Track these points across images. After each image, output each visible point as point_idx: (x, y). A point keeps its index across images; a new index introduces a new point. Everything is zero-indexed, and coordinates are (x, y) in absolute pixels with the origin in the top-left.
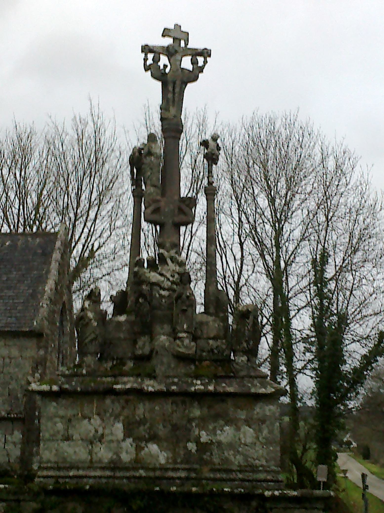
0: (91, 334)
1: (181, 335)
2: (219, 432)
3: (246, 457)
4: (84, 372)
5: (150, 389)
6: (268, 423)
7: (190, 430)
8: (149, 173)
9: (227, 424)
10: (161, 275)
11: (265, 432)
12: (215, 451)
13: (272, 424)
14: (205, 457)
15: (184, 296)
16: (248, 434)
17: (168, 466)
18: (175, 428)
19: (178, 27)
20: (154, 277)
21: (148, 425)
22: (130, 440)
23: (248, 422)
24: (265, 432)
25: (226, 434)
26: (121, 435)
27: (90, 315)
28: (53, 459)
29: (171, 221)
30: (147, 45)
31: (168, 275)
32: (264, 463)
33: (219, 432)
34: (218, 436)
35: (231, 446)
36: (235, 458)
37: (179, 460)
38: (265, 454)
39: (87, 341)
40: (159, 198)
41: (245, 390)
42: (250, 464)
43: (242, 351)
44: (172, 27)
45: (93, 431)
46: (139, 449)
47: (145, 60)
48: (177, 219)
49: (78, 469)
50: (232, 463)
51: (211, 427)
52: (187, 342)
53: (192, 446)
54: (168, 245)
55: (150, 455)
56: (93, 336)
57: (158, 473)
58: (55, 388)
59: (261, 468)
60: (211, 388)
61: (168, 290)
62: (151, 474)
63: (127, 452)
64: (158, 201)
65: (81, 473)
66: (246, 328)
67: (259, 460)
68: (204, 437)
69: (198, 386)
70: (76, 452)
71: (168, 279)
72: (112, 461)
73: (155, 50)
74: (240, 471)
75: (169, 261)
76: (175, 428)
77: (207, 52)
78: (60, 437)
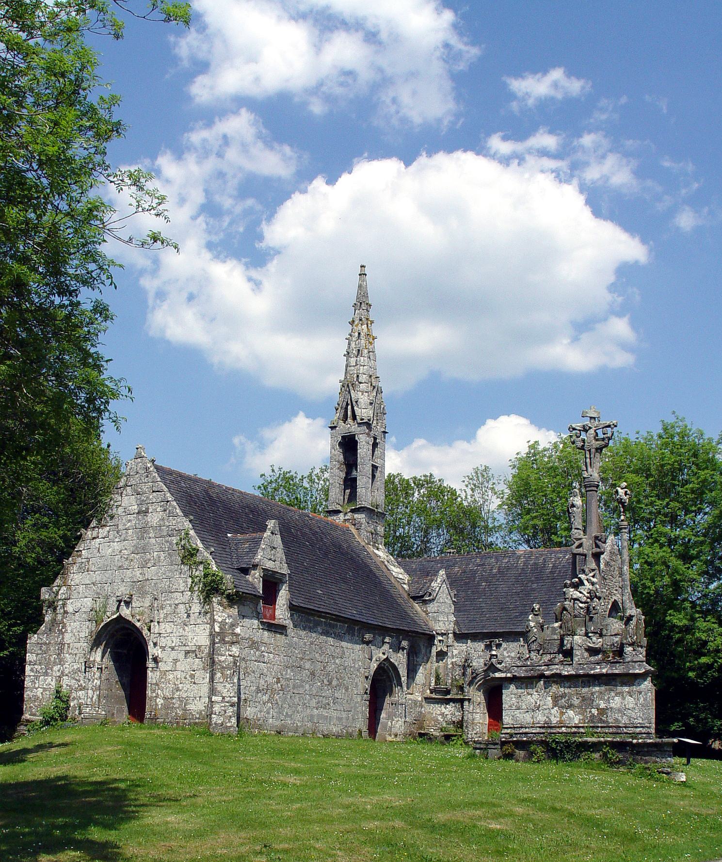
3: (630, 718)
5: (566, 673)
10: (581, 592)
13: (646, 694)
16: (630, 701)
18: (584, 699)
20: (575, 594)
22: (556, 708)
23: (630, 694)
25: (616, 702)
26: (551, 705)
27: (532, 624)
28: (511, 722)
31: (585, 593)
35: (619, 710)
40: (582, 536)
46: (562, 714)
50: (620, 722)
52: (594, 639)
53: (595, 711)
57: (574, 730)
58: (509, 675)
60: (604, 671)
61: (584, 603)
62: (569, 730)
68: (602, 705)
72: (546, 723)
75: (586, 582)
76: (584, 699)
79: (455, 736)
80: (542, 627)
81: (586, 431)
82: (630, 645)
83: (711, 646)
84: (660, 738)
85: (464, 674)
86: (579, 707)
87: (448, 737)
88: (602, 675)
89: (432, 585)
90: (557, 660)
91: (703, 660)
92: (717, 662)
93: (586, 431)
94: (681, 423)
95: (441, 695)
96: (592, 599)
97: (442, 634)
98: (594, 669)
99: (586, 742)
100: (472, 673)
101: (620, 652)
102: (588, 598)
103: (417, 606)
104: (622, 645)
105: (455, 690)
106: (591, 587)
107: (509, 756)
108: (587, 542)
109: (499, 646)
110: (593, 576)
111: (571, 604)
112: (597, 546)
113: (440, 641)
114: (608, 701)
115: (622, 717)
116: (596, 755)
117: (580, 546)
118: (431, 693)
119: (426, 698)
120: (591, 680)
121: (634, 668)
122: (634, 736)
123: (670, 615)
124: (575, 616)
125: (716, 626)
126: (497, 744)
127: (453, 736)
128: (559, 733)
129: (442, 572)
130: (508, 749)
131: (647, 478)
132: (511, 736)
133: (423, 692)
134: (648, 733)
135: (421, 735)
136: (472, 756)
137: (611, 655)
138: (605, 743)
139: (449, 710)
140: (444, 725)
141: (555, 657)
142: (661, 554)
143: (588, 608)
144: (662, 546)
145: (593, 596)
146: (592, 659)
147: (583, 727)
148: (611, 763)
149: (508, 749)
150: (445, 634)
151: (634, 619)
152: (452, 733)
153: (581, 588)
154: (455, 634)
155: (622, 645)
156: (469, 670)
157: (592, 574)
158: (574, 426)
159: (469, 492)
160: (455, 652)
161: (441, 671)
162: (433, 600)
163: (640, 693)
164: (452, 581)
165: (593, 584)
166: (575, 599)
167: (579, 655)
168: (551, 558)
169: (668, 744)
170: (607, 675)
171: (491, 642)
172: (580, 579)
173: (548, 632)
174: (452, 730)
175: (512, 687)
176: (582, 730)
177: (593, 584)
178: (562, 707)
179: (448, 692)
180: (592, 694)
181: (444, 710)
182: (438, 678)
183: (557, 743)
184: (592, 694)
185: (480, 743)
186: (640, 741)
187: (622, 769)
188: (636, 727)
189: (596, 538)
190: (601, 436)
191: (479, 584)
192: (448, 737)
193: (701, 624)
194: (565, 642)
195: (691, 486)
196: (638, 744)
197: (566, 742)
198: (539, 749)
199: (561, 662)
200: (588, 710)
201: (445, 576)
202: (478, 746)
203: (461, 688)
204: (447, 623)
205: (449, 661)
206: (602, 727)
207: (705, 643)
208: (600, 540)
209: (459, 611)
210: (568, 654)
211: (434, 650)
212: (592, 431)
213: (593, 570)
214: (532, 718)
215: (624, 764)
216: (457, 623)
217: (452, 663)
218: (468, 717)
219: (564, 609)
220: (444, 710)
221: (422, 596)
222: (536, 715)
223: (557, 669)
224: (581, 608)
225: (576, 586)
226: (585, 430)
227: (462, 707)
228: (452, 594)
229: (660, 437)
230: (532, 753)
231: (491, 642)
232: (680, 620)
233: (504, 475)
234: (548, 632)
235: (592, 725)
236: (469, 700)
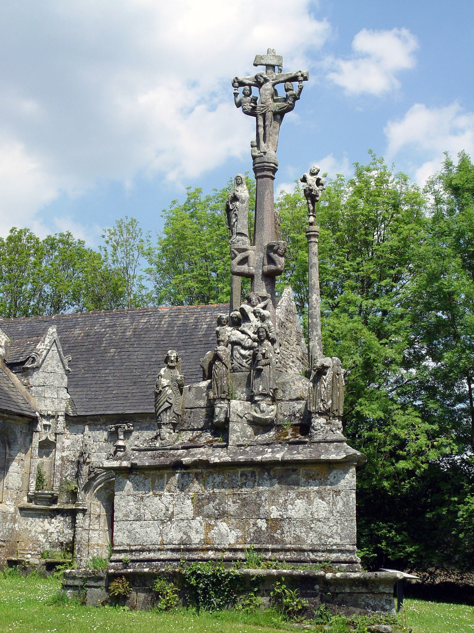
0: (164, 403)
1: (257, 398)
2: (290, 506)
3: (320, 535)
4: (158, 445)
5: (217, 460)
6: (342, 494)
7: (260, 505)
8: (234, 220)
9: (298, 497)
10: (243, 332)
11: (340, 505)
12: (286, 528)
14: (276, 535)
15: (260, 355)
16: (321, 507)
17: (238, 546)
20: (236, 335)
21: (217, 501)
24: (340, 505)
25: (298, 508)
26: (191, 514)
28: (126, 541)
29: (261, 271)
30: (236, 78)
31: (250, 333)
32: (338, 541)
33: (290, 506)
34: (289, 511)
35: (303, 522)
36: (307, 536)
37: (249, 540)
38: (339, 531)
39: (160, 410)
40: (247, 246)
41: (314, 456)
42: (323, 541)
43: (318, 413)
44: (263, 52)
45: (164, 509)
46: (209, 527)
47: (236, 95)
48: (267, 267)
49: (150, 551)
50: (304, 542)
51: (281, 501)
52: (263, 405)
53: (262, 524)
54: (254, 298)
55: (220, 534)
56: (167, 405)
57: (228, 555)
58: (125, 464)
59: (335, 547)
60: (279, 456)
61: (250, 348)
62: (220, 555)
63: (197, 532)
64: (245, 250)
65: (152, 555)
66: (323, 385)
67: (333, 539)
68: (275, 514)
69: (268, 455)
70: (150, 534)
71: (250, 337)
73: (245, 81)
74: (313, 551)
75: (251, 316)
76: (245, 503)
78: (132, 517)
79: (62, 564)
80: (180, 388)
81: (259, 84)
82: (321, 414)
83: (412, 447)
84: (370, 571)
85: (78, 475)
86: (238, 516)
87: (51, 566)
88: (275, 463)
89: (38, 347)
90: (203, 440)
91: (402, 465)
92: (419, 467)
93: (259, 84)
94: (379, 165)
95: (43, 504)
96: (260, 342)
97: (49, 417)
98: (262, 453)
99: (247, 576)
100: (90, 473)
101: (304, 427)
102: (254, 340)
103: (15, 378)
104: (307, 416)
105: (63, 498)
106: (259, 324)
107: (118, 600)
108: (256, 256)
109: (127, 434)
110: (264, 308)
111: (228, 350)
112: (271, 261)
113: (45, 426)
114: (284, 506)
115: (307, 533)
116: (262, 600)
117: (245, 261)
118: (30, 501)
119: (21, 509)
120: (257, 471)
121: (327, 451)
122: (329, 565)
123: (361, 405)
124: (234, 370)
125: (419, 420)
126: (101, 579)
127: (59, 563)
128: (203, 560)
129: (52, 330)
130: (118, 587)
131: (334, 231)
132: (126, 565)
133: (17, 500)
134: (352, 562)
135: (11, 563)
136: (59, 600)
137: (290, 431)
138: (278, 577)
139: (56, 527)
140: (47, 547)
141: (200, 436)
142: (350, 325)
143: (254, 356)
144: (351, 316)
145: (262, 336)
146: (259, 438)
147: (242, 550)
148: (289, 613)
149: (118, 587)
150: (53, 417)
151: (329, 372)
152: (58, 559)
153: (245, 327)
154: (67, 416)
155: (307, 416)
156: (85, 469)
157: (262, 304)
158: (240, 78)
159: (110, 250)
160: (67, 443)
161: (46, 470)
162: (38, 368)
163: (338, 493)
164: (67, 345)
165: (263, 319)
166: (234, 343)
167: (239, 431)
168: (206, 318)
169: (387, 581)
170: (284, 463)
171: (117, 428)
172: (242, 311)
173: (190, 395)
174: (58, 555)
175: (129, 485)
176: (240, 555)
177: (263, 319)
178: (209, 516)
179: (54, 500)
180: (258, 494)
181: (47, 526)
182: (40, 479)
183: (199, 576)
184: (258, 494)
185: (74, 578)
186: (338, 575)
187: (307, 624)
188: (331, 551)
189: (270, 248)
190: (282, 94)
191: (106, 351)
192: (51, 566)
193: (399, 418)
194: (217, 410)
195: (390, 243)
196: (336, 582)
197: (214, 575)
198: (169, 588)
199: (210, 444)
200: (251, 522)
201: (55, 335)
202: (70, 582)
203: (73, 495)
204: (56, 402)
205: (58, 455)
206: (273, 551)
207: (403, 444)
208: (276, 252)
209: (76, 386)
210: (221, 430)
211: (36, 439)
212: (268, 86)
213: (264, 298)
214: (161, 534)
215: (311, 616)
216: (72, 402)
217: (62, 458)
218: (81, 535)
219: (217, 357)
220: (47, 526)
221: (23, 363)
222: (167, 529)
223: (202, 453)
224: (244, 357)
225: (236, 323)
226: (259, 83)
227: (74, 521)
228: (66, 361)
229: (352, 183)
230: (157, 594)
231: (117, 428)
232: (373, 411)
233: (154, 232)
234: (190, 395)
235: (257, 546)
236: (84, 511)
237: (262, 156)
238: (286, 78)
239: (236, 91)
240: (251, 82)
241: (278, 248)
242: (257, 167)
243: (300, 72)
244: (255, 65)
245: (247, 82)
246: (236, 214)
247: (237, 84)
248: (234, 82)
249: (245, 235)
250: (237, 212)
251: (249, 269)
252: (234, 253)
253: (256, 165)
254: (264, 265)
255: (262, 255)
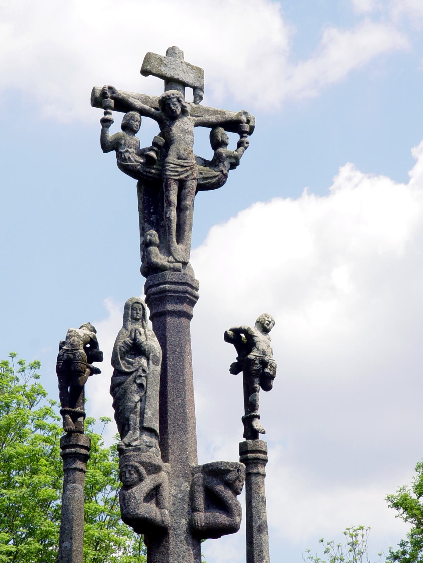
8: (136, 398)
19: (171, 52)
29: (184, 522)
30: (110, 88)
40: (158, 460)
48: (202, 517)
73: (131, 100)
77: (248, 122)
237: (179, 270)
238: (220, 118)
239: (108, 116)
240: (147, 107)
241: (238, 478)
242: (169, 291)
243: (245, 113)
244: (145, 72)
245: (139, 104)
246: (141, 386)
247: (112, 103)
248: (104, 94)
249: (156, 434)
250: (143, 381)
251: (163, 515)
252: (138, 471)
253: (167, 286)
254: (194, 509)
255: (186, 486)
